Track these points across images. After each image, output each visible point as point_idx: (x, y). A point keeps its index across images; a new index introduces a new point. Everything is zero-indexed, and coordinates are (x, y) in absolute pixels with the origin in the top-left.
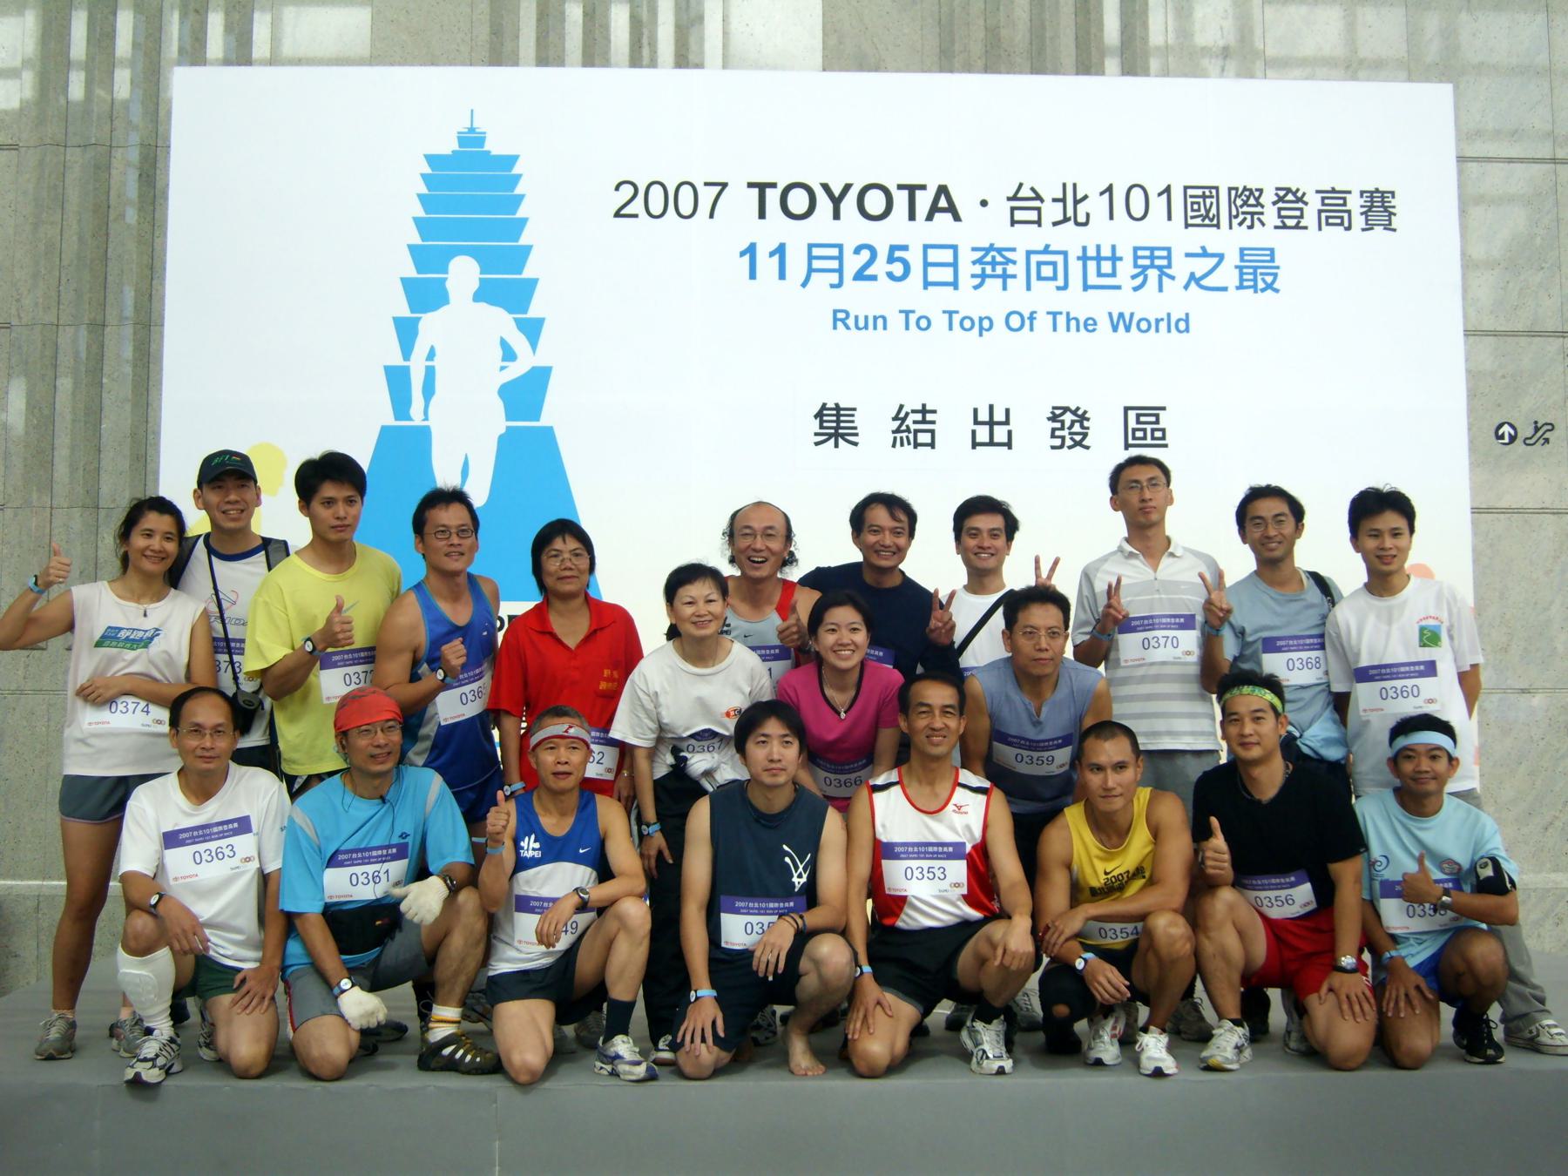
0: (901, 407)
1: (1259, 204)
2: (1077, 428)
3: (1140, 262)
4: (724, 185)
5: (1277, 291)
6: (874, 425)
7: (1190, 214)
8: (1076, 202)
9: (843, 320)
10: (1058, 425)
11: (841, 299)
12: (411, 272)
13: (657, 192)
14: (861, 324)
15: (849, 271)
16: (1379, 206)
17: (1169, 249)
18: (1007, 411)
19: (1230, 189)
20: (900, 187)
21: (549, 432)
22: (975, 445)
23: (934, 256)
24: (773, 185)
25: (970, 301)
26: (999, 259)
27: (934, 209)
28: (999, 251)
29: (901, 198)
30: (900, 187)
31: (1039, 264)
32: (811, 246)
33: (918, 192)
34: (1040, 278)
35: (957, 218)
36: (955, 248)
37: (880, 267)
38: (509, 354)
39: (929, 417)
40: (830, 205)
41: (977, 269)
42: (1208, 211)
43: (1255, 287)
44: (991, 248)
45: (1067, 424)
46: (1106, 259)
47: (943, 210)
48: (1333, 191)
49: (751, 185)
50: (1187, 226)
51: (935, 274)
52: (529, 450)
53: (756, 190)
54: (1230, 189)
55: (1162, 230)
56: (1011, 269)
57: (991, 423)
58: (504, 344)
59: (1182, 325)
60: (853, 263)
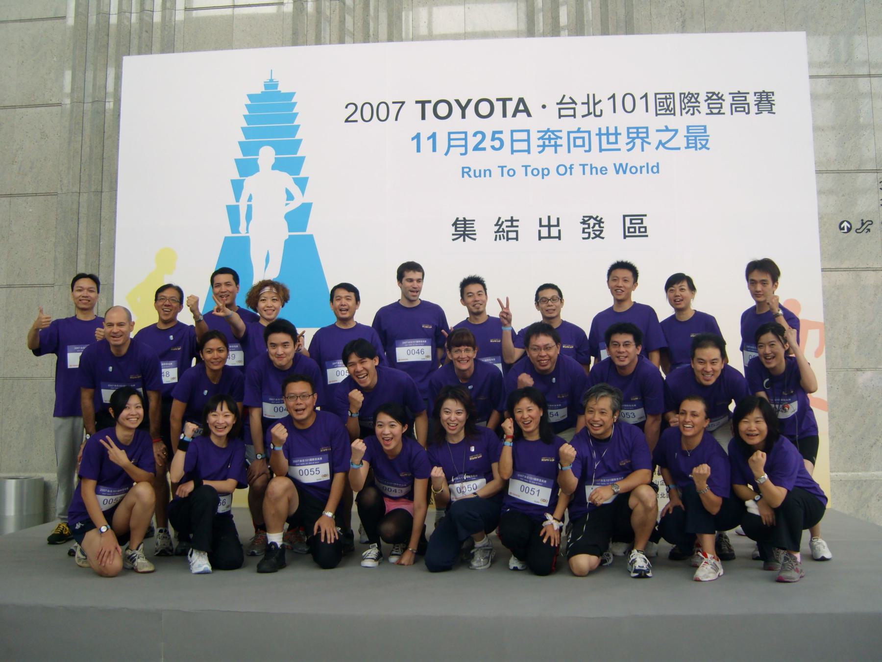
0: (499, 218)
1: (697, 101)
2: (597, 227)
3: (631, 135)
4: (403, 103)
5: (708, 149)
7: (658, 108)
8: (595, 104)
9: (467, 173)
10: (586, 226)
11: (466, 161)
13: (367, 108)
14: (477, 174)
15: (471, 146)
16: (765, 100)
17: (647, 128)
18: (558, 219)
19: (681, 94)
20: (498, 100)
21: (311, 237)
22: (540, 238)
23: (517, 136)
24: (429, 102)
25: (536, 159)
26: (552, 136)
27: (517, 111)
28: (553, 132)
29: (498, 106)
30: (498, 100)
31: (575, 138)
32: (450, 133)
33: (508, 102)
34: (575, 146)
35: (529, 115)
36: (528, 131)
37: (487, 143)
38: (290, 197)
39: (515, 224)
40: (460, 111)
41: (541, 142)
42: (668, 106)
43: (696, 147)
45: (591, 225)
47: (521, 111)
48: (739, 93)
49: (417, 102)
50: (657, 115)
51: (517, 146)
52: (301, 249)
54: (681, 94)
55: (642, 117)
56: (559, 142)
57: (549, 226)
59: (655, 169)
60: (472, 142)
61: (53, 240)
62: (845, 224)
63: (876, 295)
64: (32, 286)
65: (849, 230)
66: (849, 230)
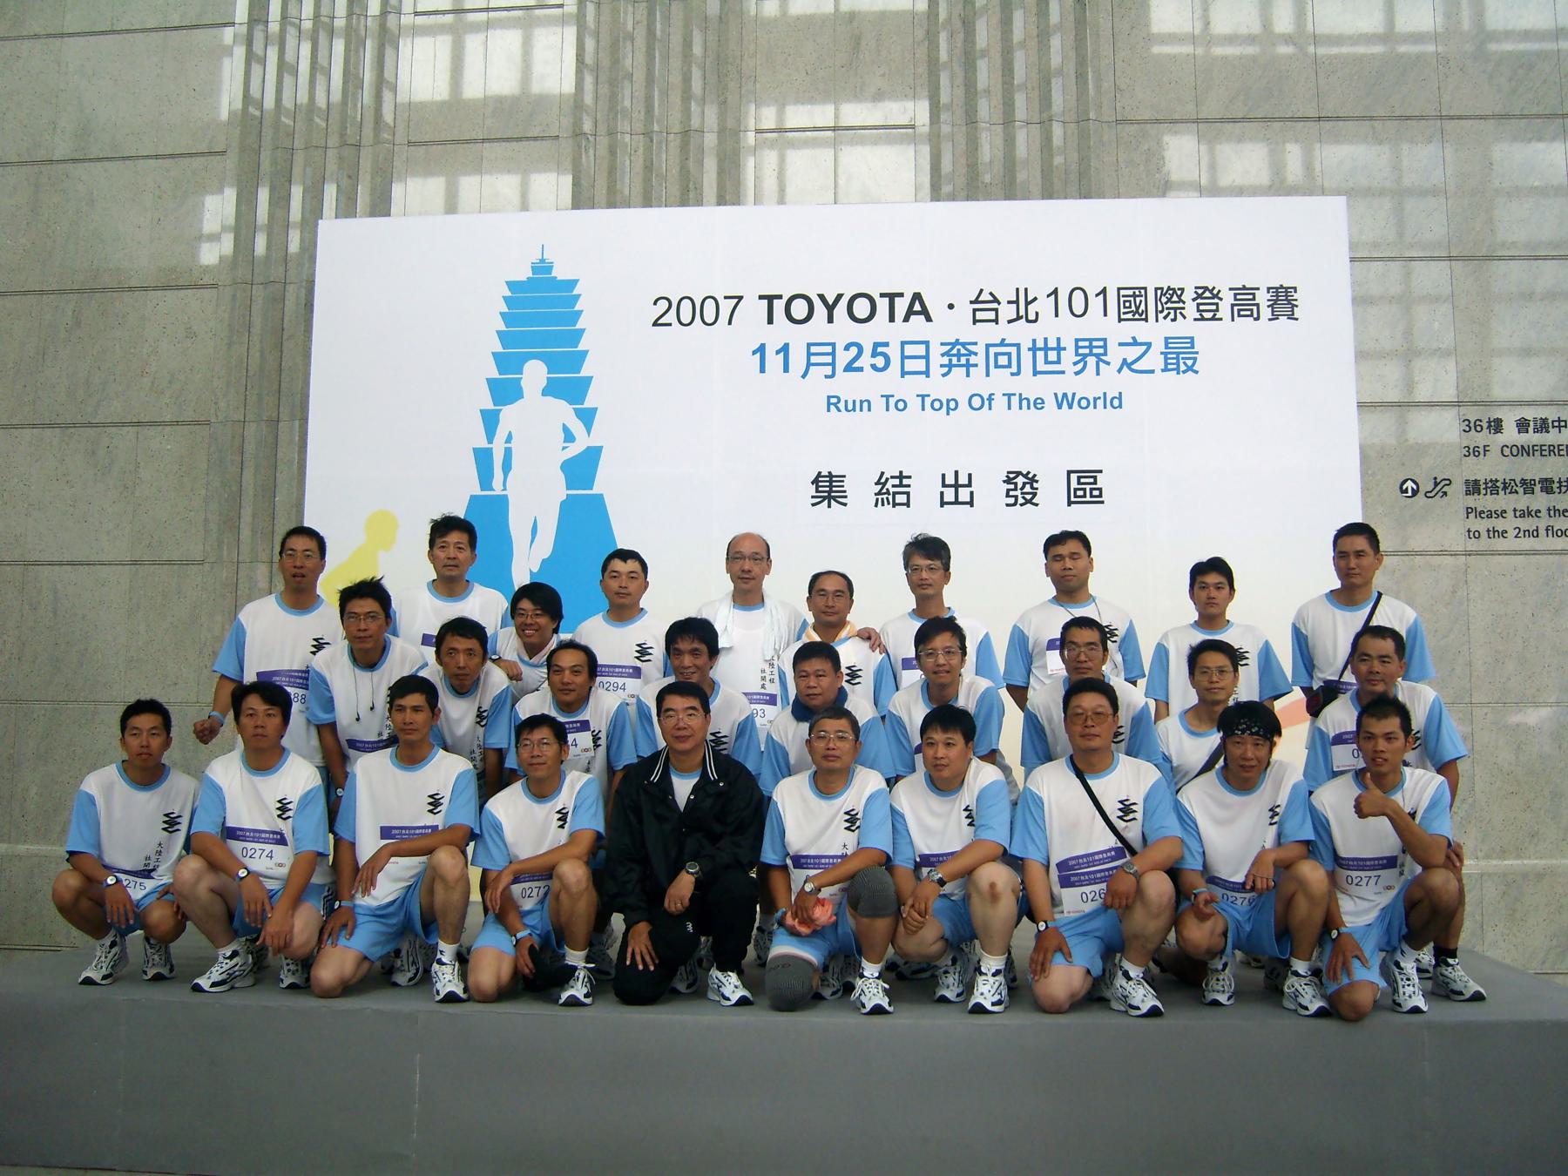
2: (1028, 489)
4: (740, 298)
8: (1027, 303)
12: (495, 374)
13: (686, 304)
15: (840, 365)
16: (1284, 300)
17: (1105, 340)
20: (882, 295)
22: (943, 504)
24: (780, 297)
25: (939, 386)
27: (910, 312)
28: (964, 345)
29: (882, 305)
30: (882, 295)
31: (996, 355)
32: (809, 345)
34: (997, 366)
35: (929, 319)
36: (927, 343)
37: (866, 360)
38: (569, 437)
39: (905, 482)
41: (945, 360)
44: (954, 345)
47: (917, 313)
48: (1244, 288)
49: (761, 297)
50: (1120, 320)
51: (910, 365)
53: (765, 302)
55: (1099, 324)
56: (973, 360)
57: (956, 486)
58: (565, 428)
59: (1116, 402)
60: (843, 358)
61: (203, 492)
62: (1409, 484)
63: (1454, 592)
64: (170, 562)
65: (1415, 493)
66: (1415, 493)
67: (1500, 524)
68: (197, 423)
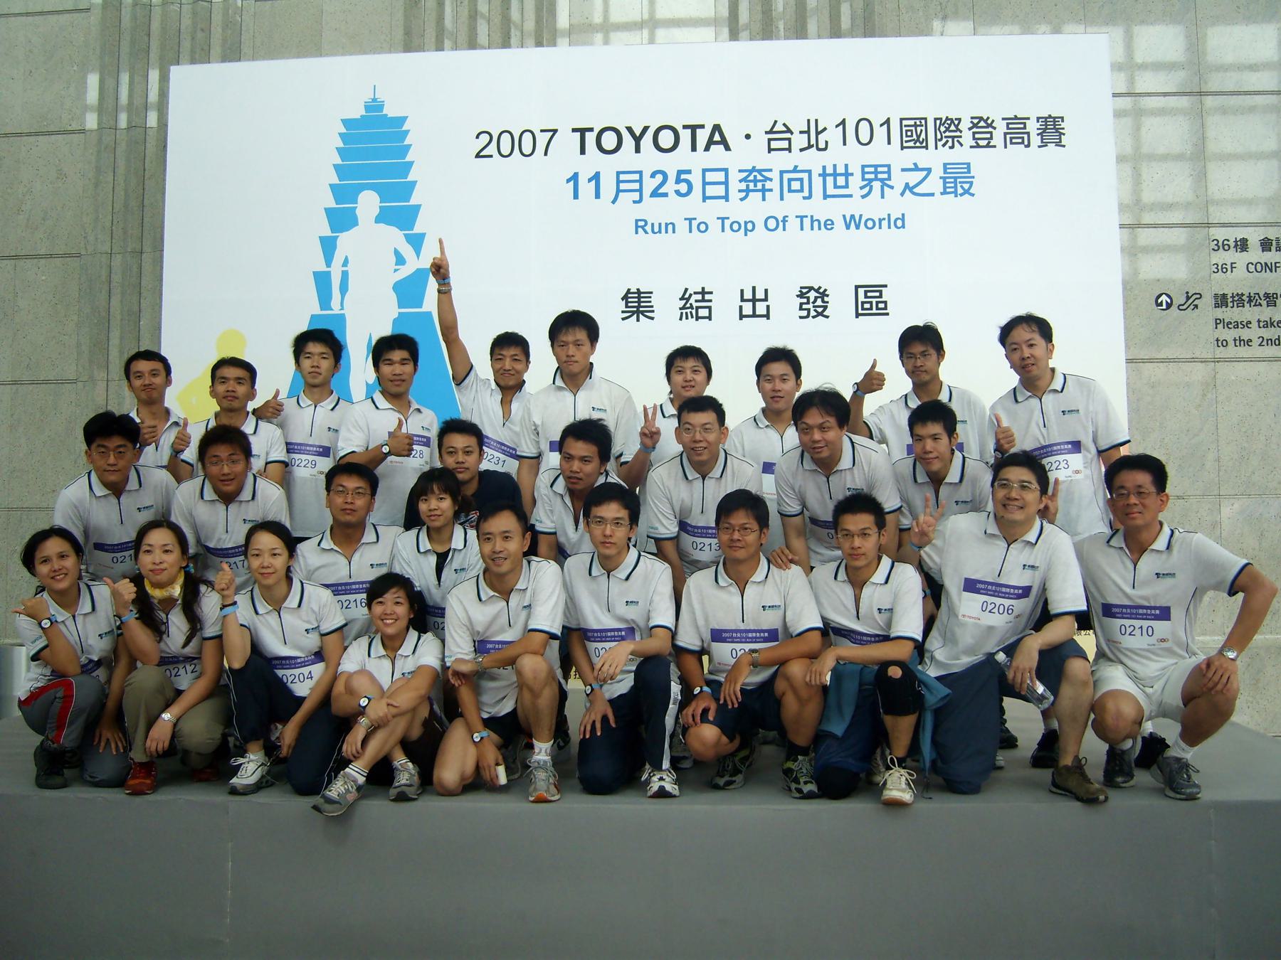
0: (686, 290)
1: (958, 130)
2: (819, 302)
3: (867, 176)
4: (555, 131)
6: (666, 304)
8: (818, 133)
9: (642, 227)
13: (506, 139)
14: (656, 229)
15: (647, 191)
16: (1052, 129)
17: (889, 166)
18: (766, 291)
20: (685, 127)
22: (742, 317)
23: (710, 177)
24: (591, 130)
25: (738, 209)
26: (759, 177)
27: (710, 142)
28: (760, 171)
29: (685, 136)
30: (685, 127)
31: (790, 180)
32: (618, 173)
34: (790, 191)
35: (727, 148)
36: (726, 170)
37: (670, 187)
38: (400, 260)
39: (707, 297)
41: (743, 186)
42: (918, 137)
44: (751, 172)
45: (812, 300)
46: (841, 175)
47: (717, 143)
48: (1016, 118)
49: (574, 130)
50: (903, 148)
51: (711, 190)
53: (578, 134)
55: (884, 152)
56: (768, 185)
57: (754, 300)
58: (397, 252)
59: (899, 223)
60: (650, 184)
61: (75, 318)
62: (1164, 298)
63: (1204, 395)
64: (46, 382)
65: (1169, 306)
66: (1169, 306)
67: (1245, 334)
68: (70, 256)
